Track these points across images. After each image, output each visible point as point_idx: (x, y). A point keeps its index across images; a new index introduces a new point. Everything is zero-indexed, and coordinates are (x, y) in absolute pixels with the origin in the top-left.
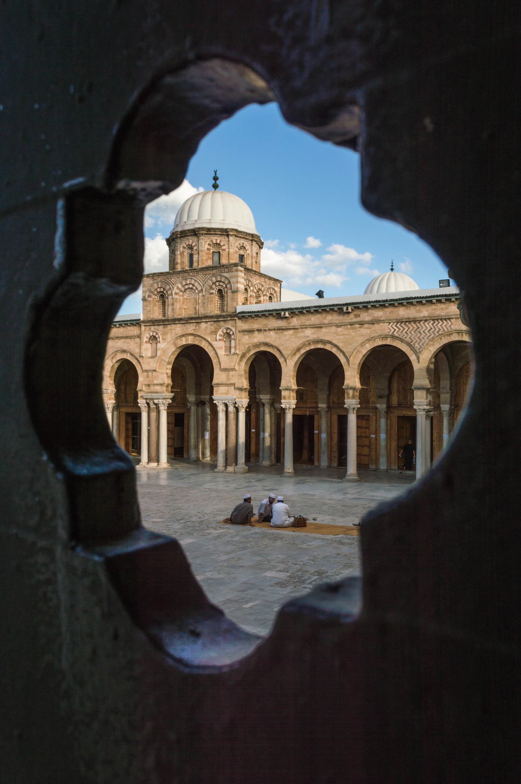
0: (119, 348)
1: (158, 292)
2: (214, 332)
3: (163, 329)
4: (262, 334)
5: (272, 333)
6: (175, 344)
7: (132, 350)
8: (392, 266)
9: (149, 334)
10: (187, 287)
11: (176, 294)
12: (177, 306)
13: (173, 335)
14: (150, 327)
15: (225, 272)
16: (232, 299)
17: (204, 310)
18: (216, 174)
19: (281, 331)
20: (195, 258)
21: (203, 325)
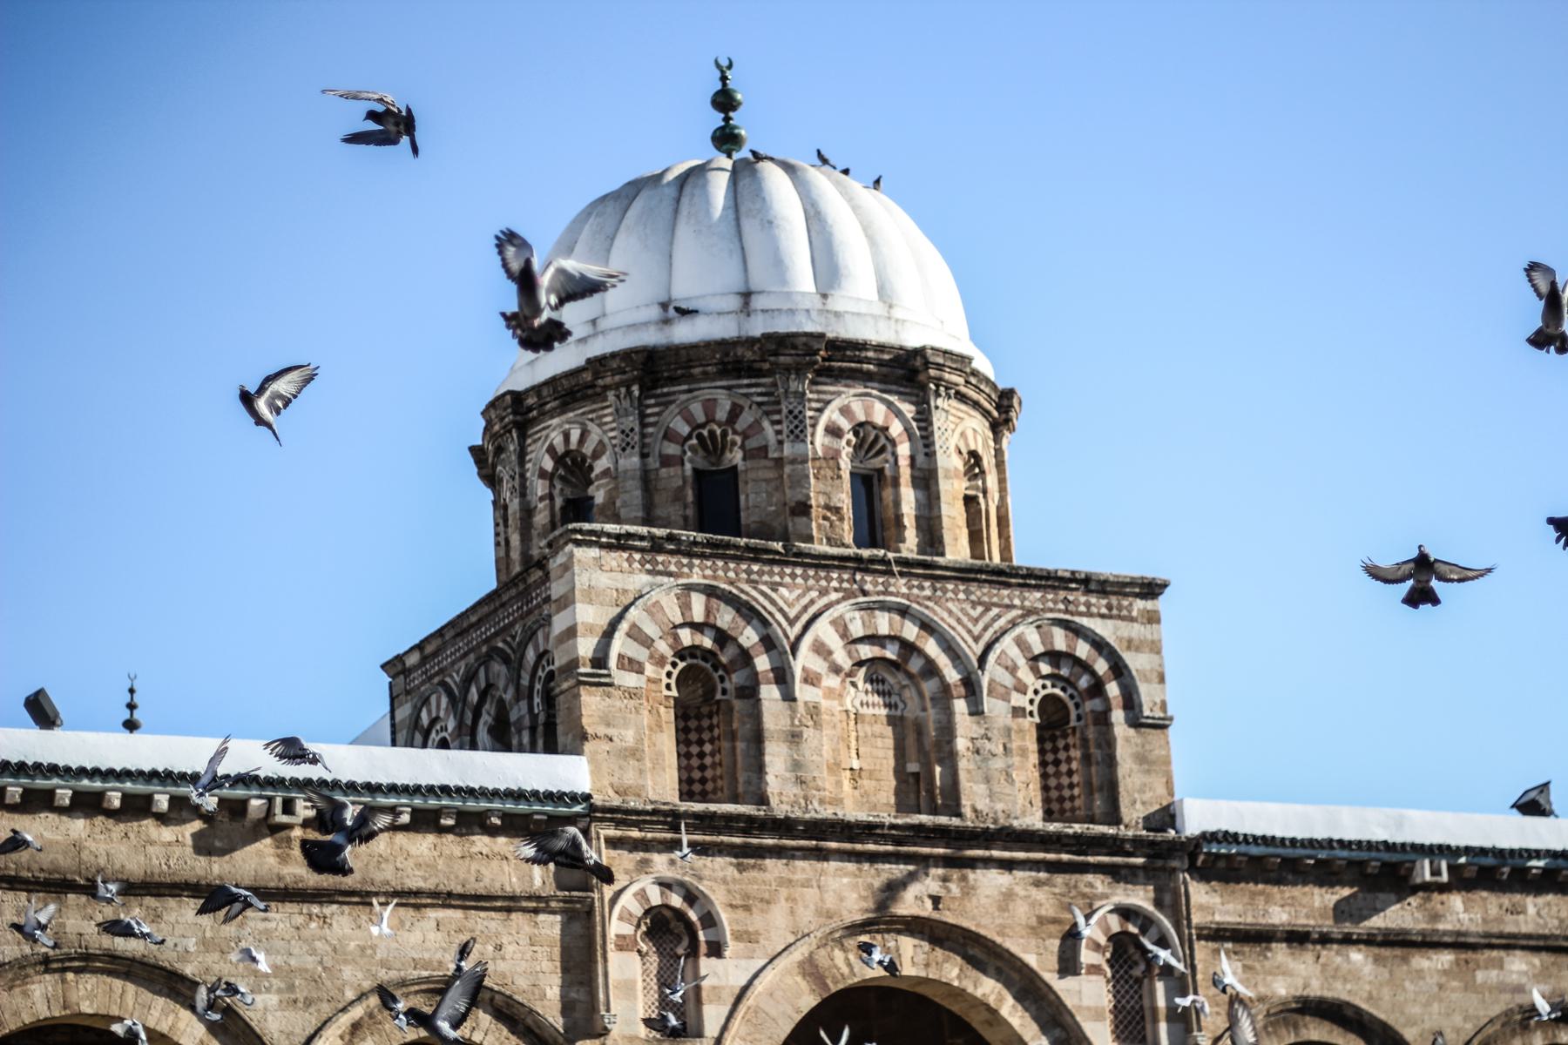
0: (416, 964)
1: (681, 654)
2: (1055, 921)
3: (732, 872)
4: (1309, 957)
5: (1357, 956)
6: (810, 969)
7: (522, 983)
8: (131, 707)
9: (642, 895)
10: (866, 651)
11: (811, 679)
12: (820, 745)
13: (807, 917)
14: (639, 855)
15: (1089, 615)
16: (1142, 759)
17: (991, 795)
18: (724, 79)
19: (1398, 952)
20: (909, 499)
21: (990, 882)
